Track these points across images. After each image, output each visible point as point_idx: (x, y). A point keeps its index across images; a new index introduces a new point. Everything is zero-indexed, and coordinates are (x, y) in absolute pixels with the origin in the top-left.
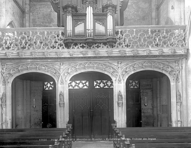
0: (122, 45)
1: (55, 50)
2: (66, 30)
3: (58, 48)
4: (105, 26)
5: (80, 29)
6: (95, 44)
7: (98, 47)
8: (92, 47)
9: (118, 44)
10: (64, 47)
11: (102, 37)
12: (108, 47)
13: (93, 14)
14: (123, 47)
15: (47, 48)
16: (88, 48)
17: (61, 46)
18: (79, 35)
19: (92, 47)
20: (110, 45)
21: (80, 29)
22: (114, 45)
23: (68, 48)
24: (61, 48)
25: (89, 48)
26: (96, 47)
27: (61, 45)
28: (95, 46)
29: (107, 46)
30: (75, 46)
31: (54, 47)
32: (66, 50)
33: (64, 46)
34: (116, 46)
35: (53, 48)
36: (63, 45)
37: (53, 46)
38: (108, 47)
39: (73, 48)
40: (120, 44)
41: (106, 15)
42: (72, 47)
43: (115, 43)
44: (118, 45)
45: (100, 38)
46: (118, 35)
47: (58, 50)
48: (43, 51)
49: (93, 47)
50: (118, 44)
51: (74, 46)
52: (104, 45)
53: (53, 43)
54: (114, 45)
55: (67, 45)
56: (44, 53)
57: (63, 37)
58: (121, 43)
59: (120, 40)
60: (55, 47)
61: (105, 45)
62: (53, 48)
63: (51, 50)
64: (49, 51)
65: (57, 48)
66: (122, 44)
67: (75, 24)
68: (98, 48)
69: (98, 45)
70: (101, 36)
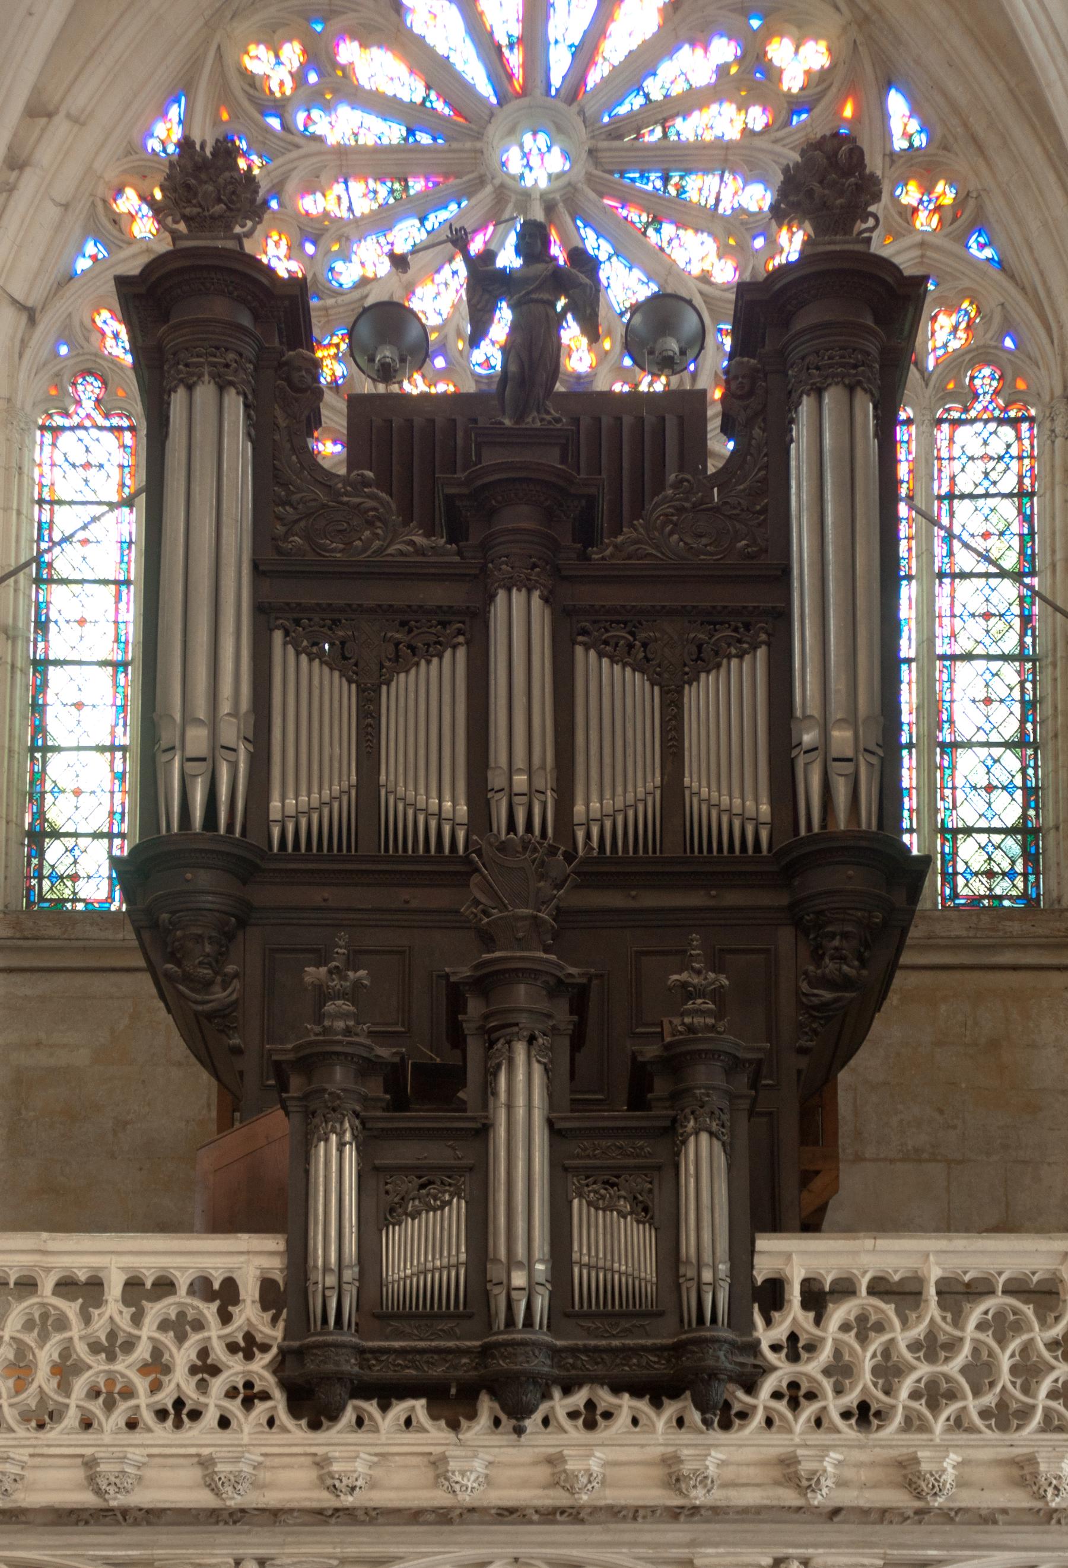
0: (809, 1410)
1: (200, 1436)
2: (298, 1256)
3: (224, 1423)
5: (423, 1251)
6: (567, 1391)
7: (591, 1418)
8: (538, 1416)
9: (777, 1395)
10: (283, 1416)
11: (628, 1332)
12: (680, 1422)
13: (550, 1123)
14: (818, 1423)
15: (119, 1416)
16: (497, 1422)
17: (248, 1403)
18: (421, 1314)
19: (533, 1422)
20: (702, 1407)
21: (423, 1251)
22: (736, 1407)
24: (248, 1424)
25: (507, 1423)
26: (573, 1415)
27: (250, 1395)
28: (560, 1405)
29: (671, 1409)
30: (384, 1408)
31: (180, 1413)
32: (296, 1434)
34: (759, 1417)
35: (178, 1425)
36: (265, 1396)
37: (179, 1404)
38: (680, 1422)
39: (360, 1422)
40: (795, 1395)
41: (671, 1136)
42: (349, 1416)
43: (751, 1388)
44: (782, 1406)
45: (616, 1343)
46: (776, 1315)
47: (225, 1437)
48: (86, 1444)
49: (546, 1422)
50: (777, 1395)
51: (371, 1407)
52: (643, 1406)
53: (180, 1380)
54: (736, 1407)
55: (312, 1395)
56: (90, 1463)
57: (274, 1320)
58: (804, 1387)
59: (794, 1357)
60: (195, 1415)
62: (178, 1425)
63: (163, 1434)
64: (137, 1447)
65: (211, 1417)
66: (811, 1396)
67: (386, 1200)
68: (590, 1425)
69: (590, 1405)
70: (625, 1324)
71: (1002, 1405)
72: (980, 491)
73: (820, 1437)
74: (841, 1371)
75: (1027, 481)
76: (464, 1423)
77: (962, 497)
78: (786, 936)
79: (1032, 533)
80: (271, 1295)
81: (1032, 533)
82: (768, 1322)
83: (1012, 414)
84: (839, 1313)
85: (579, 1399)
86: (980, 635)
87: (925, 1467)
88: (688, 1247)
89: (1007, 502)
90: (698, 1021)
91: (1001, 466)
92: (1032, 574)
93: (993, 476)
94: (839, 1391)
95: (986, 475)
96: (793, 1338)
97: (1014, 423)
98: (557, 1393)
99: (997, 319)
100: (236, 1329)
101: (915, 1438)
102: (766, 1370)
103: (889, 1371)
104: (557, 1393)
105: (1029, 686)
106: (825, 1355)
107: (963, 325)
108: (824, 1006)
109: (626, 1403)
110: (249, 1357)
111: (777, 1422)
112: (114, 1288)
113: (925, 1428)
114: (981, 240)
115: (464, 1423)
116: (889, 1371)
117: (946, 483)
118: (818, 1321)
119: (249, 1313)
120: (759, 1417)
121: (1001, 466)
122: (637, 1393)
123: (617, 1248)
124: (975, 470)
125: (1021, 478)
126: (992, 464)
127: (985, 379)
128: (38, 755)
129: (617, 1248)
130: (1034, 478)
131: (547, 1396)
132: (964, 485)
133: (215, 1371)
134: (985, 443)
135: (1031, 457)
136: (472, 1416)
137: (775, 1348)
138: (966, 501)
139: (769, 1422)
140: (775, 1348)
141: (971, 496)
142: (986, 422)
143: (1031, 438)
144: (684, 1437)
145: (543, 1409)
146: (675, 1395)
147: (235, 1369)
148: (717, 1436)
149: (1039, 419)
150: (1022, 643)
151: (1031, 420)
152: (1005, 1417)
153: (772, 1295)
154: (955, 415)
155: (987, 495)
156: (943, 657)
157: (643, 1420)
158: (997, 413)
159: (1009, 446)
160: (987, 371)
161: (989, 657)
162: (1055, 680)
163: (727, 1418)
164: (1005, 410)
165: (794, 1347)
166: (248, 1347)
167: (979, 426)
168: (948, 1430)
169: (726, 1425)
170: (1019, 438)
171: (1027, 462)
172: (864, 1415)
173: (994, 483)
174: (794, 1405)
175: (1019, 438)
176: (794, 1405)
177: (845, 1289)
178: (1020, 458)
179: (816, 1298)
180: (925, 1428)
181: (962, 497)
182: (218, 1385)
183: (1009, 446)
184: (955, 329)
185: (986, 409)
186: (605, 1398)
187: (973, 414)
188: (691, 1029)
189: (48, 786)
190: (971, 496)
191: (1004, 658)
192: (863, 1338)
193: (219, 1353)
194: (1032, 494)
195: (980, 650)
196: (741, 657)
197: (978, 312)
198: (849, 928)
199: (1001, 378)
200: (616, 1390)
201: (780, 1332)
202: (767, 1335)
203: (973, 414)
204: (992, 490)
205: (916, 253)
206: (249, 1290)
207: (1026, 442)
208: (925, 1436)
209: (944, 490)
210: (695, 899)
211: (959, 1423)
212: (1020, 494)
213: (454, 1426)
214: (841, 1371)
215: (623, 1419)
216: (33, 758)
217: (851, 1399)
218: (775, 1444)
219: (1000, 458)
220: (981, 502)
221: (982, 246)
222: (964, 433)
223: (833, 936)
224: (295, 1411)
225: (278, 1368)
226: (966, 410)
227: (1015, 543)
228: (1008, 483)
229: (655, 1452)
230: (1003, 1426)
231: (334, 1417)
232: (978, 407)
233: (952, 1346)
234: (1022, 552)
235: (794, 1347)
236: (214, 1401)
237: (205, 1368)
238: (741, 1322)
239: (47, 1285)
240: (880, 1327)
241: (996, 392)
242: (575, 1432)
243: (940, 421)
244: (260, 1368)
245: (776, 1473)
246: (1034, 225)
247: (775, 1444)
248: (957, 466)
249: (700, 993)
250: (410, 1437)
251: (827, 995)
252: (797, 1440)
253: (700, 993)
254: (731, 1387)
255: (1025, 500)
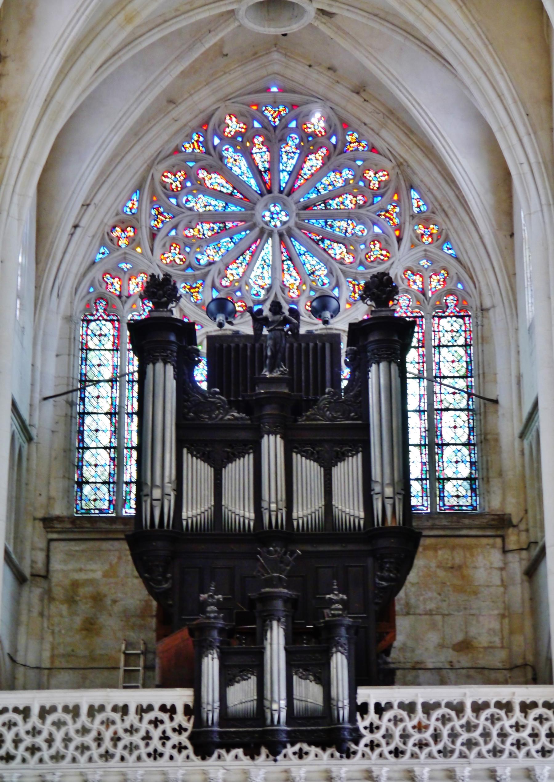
1: (163, 762)
4: (325, 681)
6: (293, 745)
7: (301, 754)
10: (192, 756)
16: (268, 756)
17: (180, 751)
23: (203, 759)
24: (180, 758)
25: (271, 757)
26: (295, 753)
27: (180, 748)
28: (290, 750)
29: (329, 751)
30: (228, 751)
31: (156, 755)
32: (196, 761)
33: (190, 751)
38: (332, 756)
39: (219, 757)
40: (372, 746)
42: (215, 755)
43: (357, 743)
51: (223, 752)
52: (319, 750)
57: (189, 720)
60: (161, 755)
61: (324, 750)
68: (301, 757)
69: (301, 750)
71: (445, 748)
72: (450, 344)
73: (381, 761)
74: (388, 736)
75: (468, 340)
76: (256, 757)
77: (443, 346)
78: (370, 562)
79: (471, 361)
80: (188, 711)
81: (471, 361)
82: (363, 718)
83: (462, 314)
84: (387, 715)
85: (296, 748)
86: (452, 401)
87: (417, 773)
88: (334, 693)
89: (461, 349)
90: (336, 612)
91: (458, 335)
92: (471, 377)
93: (455, 338)
94: (388, 744)
95: (452, 337)
96: (371, 724)
97: (463, 317)
98: (289, 746)
99: (455, 278)
100: (175, 724)
101: (415, 761)
102: (361, 736)
103: (405, 737)
104: (289, 746)
105: (471, 421)
106: (382, 731)
107: (442, 280)
108: (384, 588)
109: (313, 750)
110: (180, 733)
111: (366, 756)
112: (132, 709)
113: (417, 757)
114: (449, 246)
115: (256, 757)
116: (405, 737)
117: (437, 341)
118: (380, 718)
119: (180, 718)
120: (359, 754)
121: (458, 335)
122: (317, 746)
123: (309, 693)
124: (448, 336)
125: (466, 338)
126: (454, 334)
127: (451, 300)
128: (81, 451)
129: (309, 693)
130: (471, 339)
131: (285, 747)
132: (444, 342)
133: (168, 738)
134: (452, 325)
135: (470, 331)
136: (259, 754)
137: (365, 728)
138: (445, 348)
139: (363, 755)
140: (365, 728)
141: (447, 346)
142: (451, 317)
143: (469, 324)
144: (333, 761)
145: (284, 751)
146: (330, 746)
147: (175, 738)
148: (345, 761)
149: (472, 316)
150: (468, 404)
151: (469, 316)
152: (445, 753)
153: (363, 709)
154: (440, 314)
155: (453, 346)
156: (437, 410)
157: (319, 755)
158: (456, 313)
159: (461, 326)
160: (451, 297)
161: (455, 410)
162: (480, 420)
163: (349, 754)
164: (459, 312)
165: (372, 728)
166: (180, 730)
167: (449, 319)
168: (426, 758)
169: (348, 757)
170: (465, 324)
171: (468, 333)
172: (397, 753)
173: (456, 341)
174: (372, 749)
175: (465, 324)
176: (372, 749)
177: (389, 706)
178: (465, 331)
179: (380, 709)
180: (417, 757)
181: (443, 346)
182: (169, 744)
183: (461, 326)
184: (439, 281)
185: (452, 312)
186: (305, 747)
187: (447, 314)
188: (334, 615)
189: (84, 463)
190: (447, 346)
191: (461, 410)
192: (396, 725)
193: (169, 733)
194: (470, 346)
195: (451, 407)
196: (352, 456)
197: (448, 274)
198: (392, 560)
199: (457, 300)
200: (310, 744)
201: (367, 723)
202: (362, 724)
203: (447, 314)
204: (455, 344)
205: (424, 253)
206: (180, 709)
207: (468, 325)
208: (417, 760)
209: (436, 344)
210: (337, 548)
211: (430, 755)
212: (466, 346)
213: (253, 758)
214: (388, 736)
215: (312, 756)
216: (79, 452)
217: (392, 747)
218: (365, 764)
219: (457, 332)
220: (451, 348)
221: (449, 249)
222: (443, 321)
223: (386, 563)
224: (196, 753)
225: (190, 738)
226: (444, 312)
227: (464, 364)
228: (461, 341)
229: (323, 767)
230: (445, 756)
231: (210, 755)
232: (449, 311)
233: (427, 727)
234: (467, 368)
235: (372, 728)
236: (168, 751)
237: (165, 738)
238: (352, 719)
239: (109, 708)
240: (401, 720)
241: (456, 306)
242: (295, 760)
243: (434, 316)
244: (184, 738)
245: (365, 775)
246: (468, 245)
247: (365, 764)
248: (441, 334)
249: (337, 602)
250: (237, 763)
251: (384, 584)
252: (373, 762)
253: (337, 602)
254: (350, 743)
255: (468, 347)
